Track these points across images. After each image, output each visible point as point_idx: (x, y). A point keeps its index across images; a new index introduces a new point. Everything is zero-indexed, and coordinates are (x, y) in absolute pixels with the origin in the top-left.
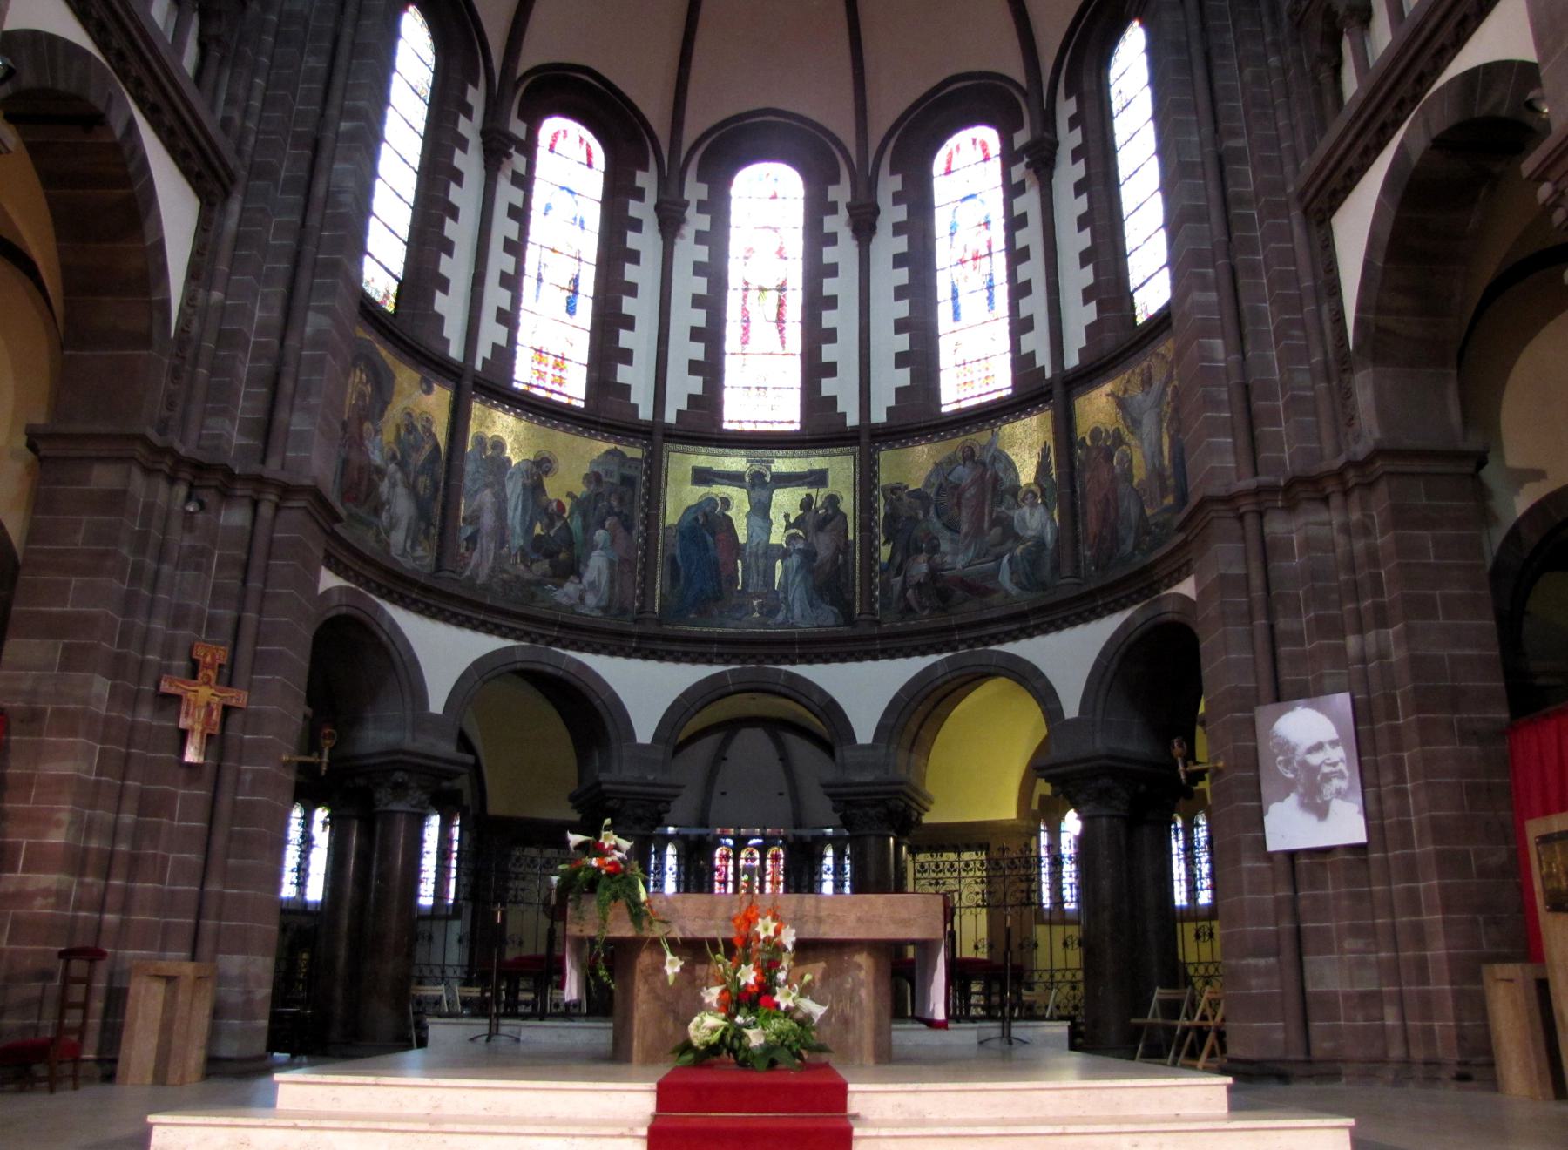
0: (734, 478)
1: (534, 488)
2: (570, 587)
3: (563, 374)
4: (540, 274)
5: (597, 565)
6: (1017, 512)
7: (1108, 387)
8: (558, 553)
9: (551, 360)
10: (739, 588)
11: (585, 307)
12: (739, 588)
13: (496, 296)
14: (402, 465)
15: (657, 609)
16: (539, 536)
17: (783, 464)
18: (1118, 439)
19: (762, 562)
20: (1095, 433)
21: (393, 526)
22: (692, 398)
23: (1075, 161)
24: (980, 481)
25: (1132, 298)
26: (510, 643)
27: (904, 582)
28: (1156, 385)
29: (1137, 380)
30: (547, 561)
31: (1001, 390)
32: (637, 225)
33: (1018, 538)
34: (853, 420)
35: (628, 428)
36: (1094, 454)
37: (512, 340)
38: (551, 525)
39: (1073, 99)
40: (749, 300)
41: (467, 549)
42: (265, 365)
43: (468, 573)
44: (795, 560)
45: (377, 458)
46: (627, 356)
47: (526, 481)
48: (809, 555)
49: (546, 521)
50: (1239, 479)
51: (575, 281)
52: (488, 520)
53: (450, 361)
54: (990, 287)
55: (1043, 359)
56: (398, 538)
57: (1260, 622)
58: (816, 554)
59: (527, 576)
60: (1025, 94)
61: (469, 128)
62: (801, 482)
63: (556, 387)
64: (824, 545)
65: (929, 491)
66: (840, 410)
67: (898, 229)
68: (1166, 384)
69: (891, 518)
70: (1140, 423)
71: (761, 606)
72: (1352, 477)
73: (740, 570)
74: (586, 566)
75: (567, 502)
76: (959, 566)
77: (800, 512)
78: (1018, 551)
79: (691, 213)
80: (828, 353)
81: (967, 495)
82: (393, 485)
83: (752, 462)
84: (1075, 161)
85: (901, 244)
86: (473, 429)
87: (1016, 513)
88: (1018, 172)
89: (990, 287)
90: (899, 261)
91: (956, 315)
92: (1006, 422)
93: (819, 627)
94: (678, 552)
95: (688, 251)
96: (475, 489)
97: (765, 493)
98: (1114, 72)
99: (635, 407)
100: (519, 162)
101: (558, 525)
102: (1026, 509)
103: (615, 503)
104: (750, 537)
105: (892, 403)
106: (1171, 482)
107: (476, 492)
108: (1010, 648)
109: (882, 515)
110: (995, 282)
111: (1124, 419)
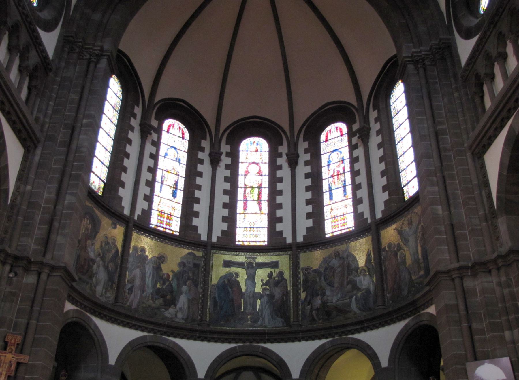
0: (240, 265)
1: (158, 268)
2: (172, 310)
3: (171, 222)
4: (162, 181)
5: (183, 301)
6: (358, 278)
7: (394, 226)
8: (167, 296)
9: (166, 216)
10: (242, 310)
11: (180, 195)
12: (242, 310)
13: (144, 190)
14: (103, 258)
15: (208, 319)
16: (159, 288)
17: (260, 259)
18: (399, 247)
19: (252, 299)
20: (390, 245)
21: (97, 284)
22: (223, 232)
23: (377, 135)
25: (403, 190)
26: (145, 334)
27: (311, 308)
28: (414, 224)
29: (406, 223)
30: (162, 299)
31: (350, 228)
32: (201, 162)
33: (359, 289)
34: (289, 240)
35: (197, 244)
36: (389, 253)
37: (150, 208)
38: (164, 284)
39: (376, 111)
40: (247, 192)
41: (128, 293)
42: (47, 216)
43: (128, 304)
44: (266, 299)
45: (92, 255)
46: (197, 215)
47: (154, 266)
48: (271, 297)
49: (162, 282)
50: (451, 263)
51: (176, 184)
52: (138, 282)
53: (125, 216)
54: (344, 186)
55: (367, 215)
56: (99, 289)
57: (465, 325)
58: (274, 296)
59: (154, 305)
60: (357, 110)
61: (135, 123)
62: (267, 266)
63: (168, 227)
64: (278, 293)
65: (321, 270)
66: (284, 236)
67: (307, 163)
68: (418, 224)
69: (305, 281)
70: (408, 241)
71: (251, 318)
72: (500, 262)
73: (243, 303)
74: (178, 301)
75: (171, 274)
76: (334, 301)
77: (268, 279)
78: (359, 294)
79: (223, 157)
80: (279, 213)
81: (337, 271)
82: (98, 266)
83: (248, 258)
84: (377, 135)
85: (308, 169)
86: (133, 243)
87: (357, 279)
88: (355, 140)
89: (344, 186)
90: (307, 176)
91: (331, 198)
92: (352, 241)
93: (276, 327)
94: (217, 295)
95: (222, 172)
96: (133, 268)
97: (253, 271)
98: (392, 100)
99: (200, 235)
100: (155, 136)
101: (167, 284)
102: (362, 277)
103: (191, 275)
104: (247, 289)
105: (305, 233)
106: (422, 265)
107: (133, 270)
108: (357, 336)
109: (302, 279)
110: (347, 184)
111: (402, 239)
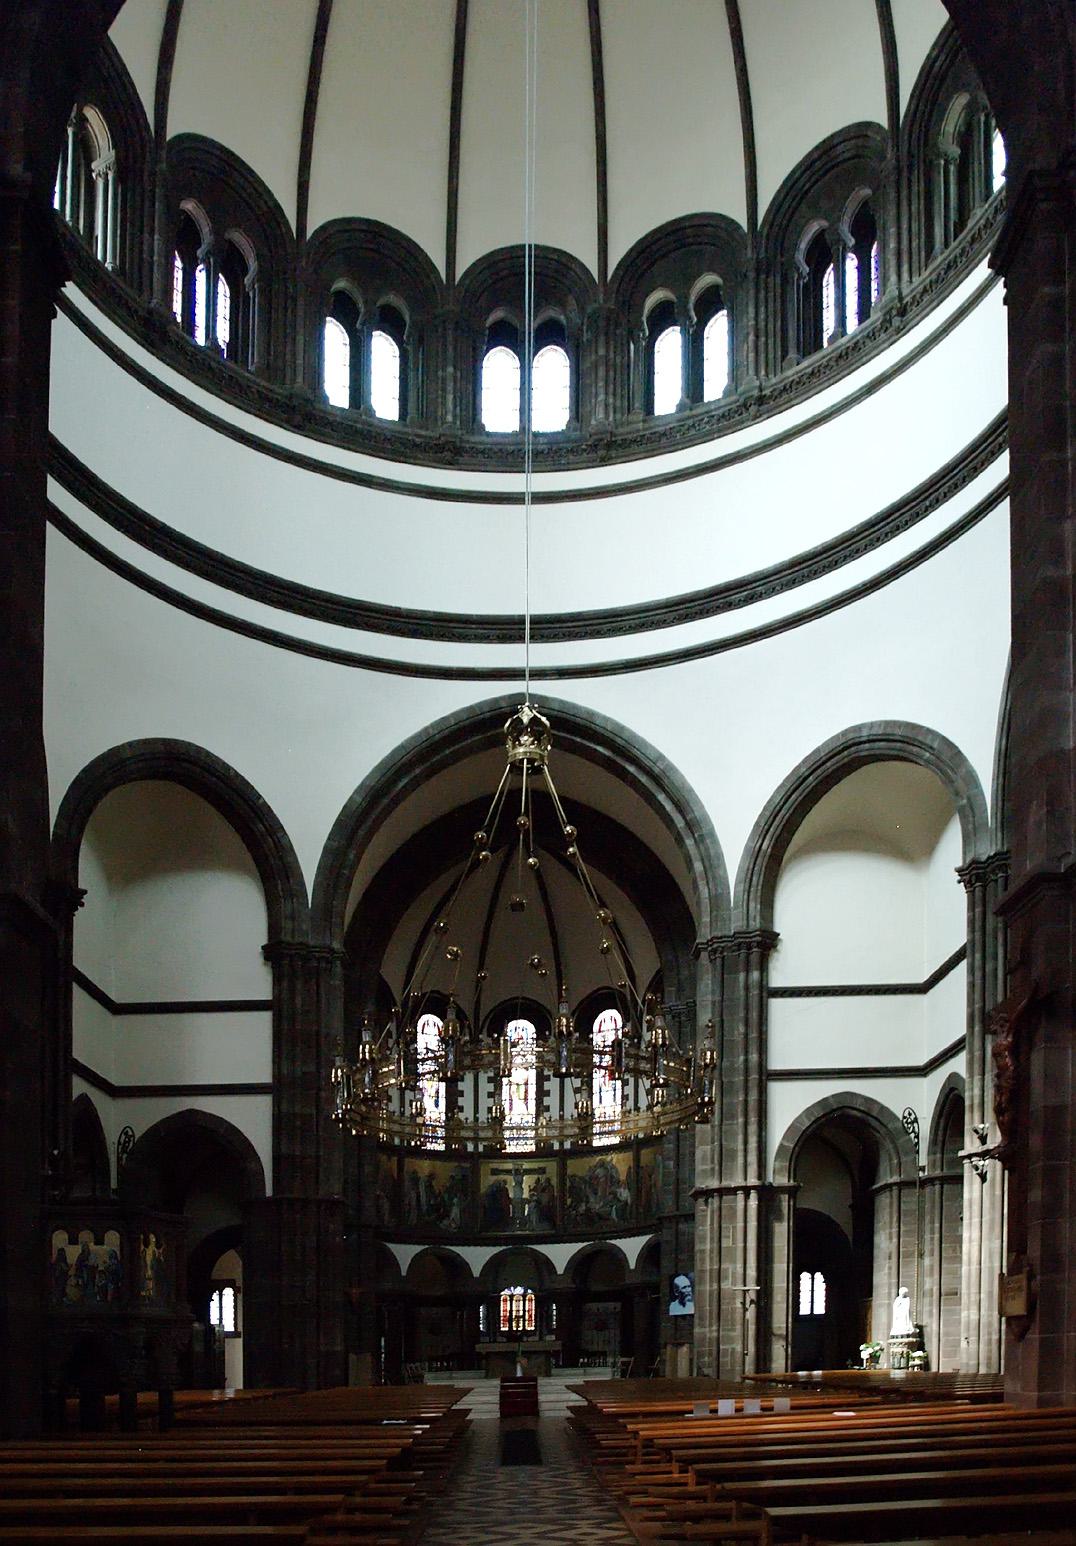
0: (508, 1172)
1: (429, 1186)
17: (526, 1165)
33: (619, 1200)
44: (533, 1204)
48: (538, 1202)
52: (414, 1203)
64: (545, 1199)
69: (572, 1187)
102: (622, 1190)
104: (515, 1195)
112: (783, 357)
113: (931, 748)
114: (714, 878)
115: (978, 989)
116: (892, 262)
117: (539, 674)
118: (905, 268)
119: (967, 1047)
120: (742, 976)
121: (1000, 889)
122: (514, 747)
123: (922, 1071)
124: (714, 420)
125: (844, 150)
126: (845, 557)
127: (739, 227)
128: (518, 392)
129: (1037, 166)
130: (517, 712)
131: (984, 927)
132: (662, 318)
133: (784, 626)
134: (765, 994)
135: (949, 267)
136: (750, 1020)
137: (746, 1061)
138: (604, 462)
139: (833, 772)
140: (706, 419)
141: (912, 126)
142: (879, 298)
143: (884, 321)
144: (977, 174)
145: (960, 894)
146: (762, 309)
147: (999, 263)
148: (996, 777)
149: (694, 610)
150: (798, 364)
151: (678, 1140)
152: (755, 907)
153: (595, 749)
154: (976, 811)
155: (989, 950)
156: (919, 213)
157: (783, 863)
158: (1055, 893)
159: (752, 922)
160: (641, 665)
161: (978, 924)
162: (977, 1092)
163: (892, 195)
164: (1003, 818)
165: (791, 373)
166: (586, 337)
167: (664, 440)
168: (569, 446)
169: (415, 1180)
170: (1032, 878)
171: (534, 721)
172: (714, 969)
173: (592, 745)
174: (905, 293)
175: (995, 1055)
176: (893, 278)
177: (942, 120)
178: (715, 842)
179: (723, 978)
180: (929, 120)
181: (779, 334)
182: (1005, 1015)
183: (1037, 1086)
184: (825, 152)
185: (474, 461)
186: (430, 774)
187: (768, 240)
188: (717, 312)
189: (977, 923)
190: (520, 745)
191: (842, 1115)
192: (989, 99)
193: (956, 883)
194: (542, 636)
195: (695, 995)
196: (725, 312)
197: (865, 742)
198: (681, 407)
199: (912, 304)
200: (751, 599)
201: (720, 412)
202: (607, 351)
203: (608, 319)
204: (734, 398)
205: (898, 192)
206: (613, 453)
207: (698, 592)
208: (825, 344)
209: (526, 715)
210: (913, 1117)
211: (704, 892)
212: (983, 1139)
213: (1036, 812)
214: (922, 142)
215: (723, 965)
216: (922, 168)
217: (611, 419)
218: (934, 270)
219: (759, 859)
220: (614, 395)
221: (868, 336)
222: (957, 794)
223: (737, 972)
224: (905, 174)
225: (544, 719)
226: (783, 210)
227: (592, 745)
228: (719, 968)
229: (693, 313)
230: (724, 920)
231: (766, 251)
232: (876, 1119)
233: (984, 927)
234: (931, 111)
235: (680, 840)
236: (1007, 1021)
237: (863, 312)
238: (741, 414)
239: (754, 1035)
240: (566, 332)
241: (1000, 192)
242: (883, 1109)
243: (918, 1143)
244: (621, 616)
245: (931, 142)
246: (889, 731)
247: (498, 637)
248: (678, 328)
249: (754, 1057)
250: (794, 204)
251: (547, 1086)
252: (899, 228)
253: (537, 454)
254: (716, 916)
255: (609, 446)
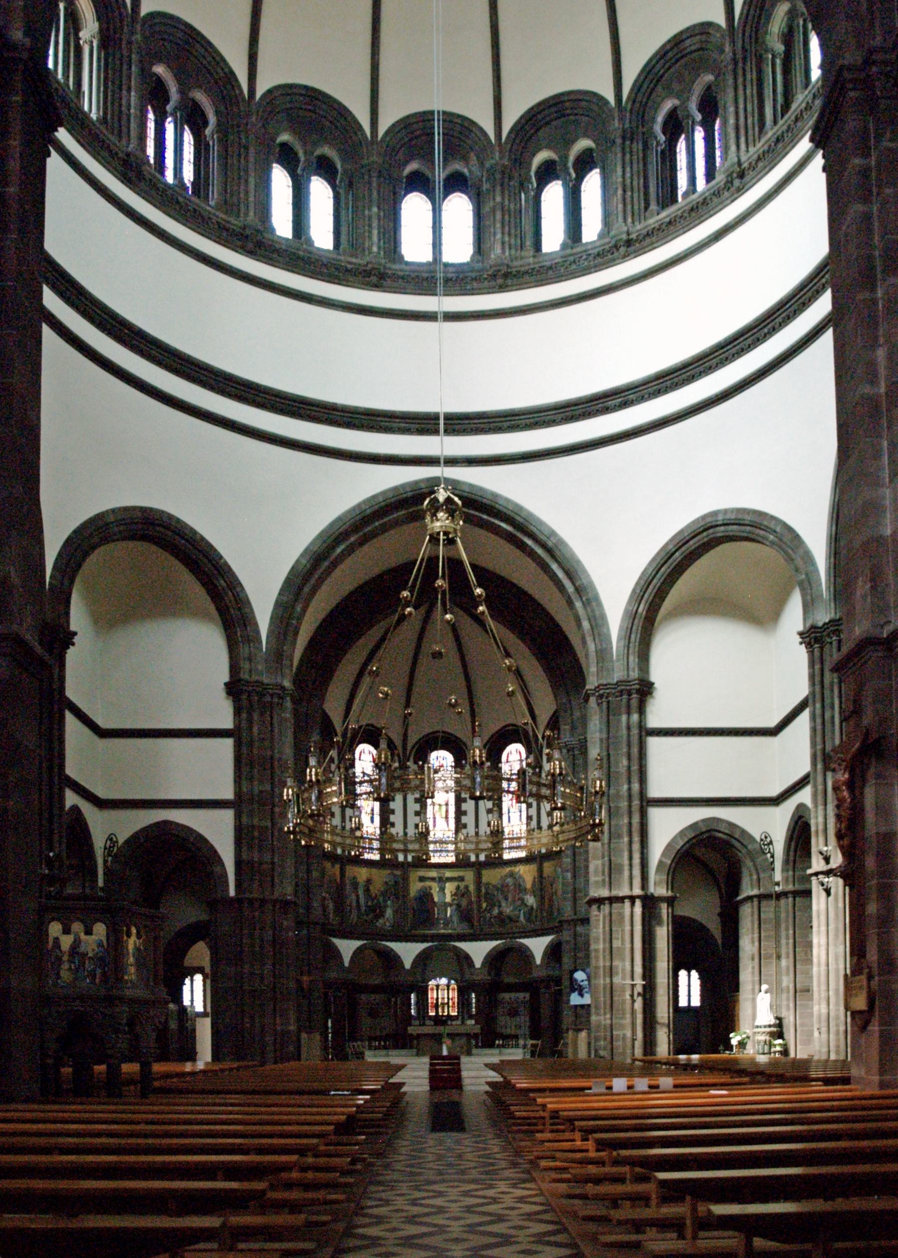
0: (433, 879)
1: (367, 890)
2: (381, 921)
5: (389, 913)
17: (448, 874)
24: (515, 884)
33: (526, 906)
44: (454, 907)
48: (459, 905)
52: (354, 904)
64: (464, 902)
69: (487, 893)
78: (526, 909)
112: (646, 208)
113: (775, 531)
114: (599, 635)
115: (819, 733)
116: (732, 135)
117: (452, 462)
118: (743, 140)
119: (811, 782)
120: (624, 718)
121: (835, 650)
122: (432, 521)
123: (776, 801)
124: (591, 258)
125: (691, 44)
126: (701, 373)
127: (607, 102)
128: (431, 230)
129: (846, 63)
130: (434, 492)
131: (822, 682)
132: (548, 173)
133: (652, 428)
134: (643, 734)
135: (778, 140)
136: (632, 755)
137: (629, 789)
138: (502, 288)
139: (695, 549)
140: (584, 257)
141: (745, 26)
142: (722, 164)
143: (727, 182)
144: (798, 68)
145: (802, 653)
146: (628, 169)
147: (818, 138)
148: (829, 557)
149: (577, 413)
150: (658, 214)
151: (574, 854)
152: (633, 660)
153: (499, 526)
154: (814, 585)
155: (827, 701)
156: (752, 96)
157: (656, 624)
158: (880, 654)
159: (631, 673)
160: (535, 457)
161: (818, 679)
162: (821, 819)
163: (731, 81)
164: (835, 591)
165: (653, 221)
166: (485, 186)
167: (550, 272)
168: (474, 275)
169: (355, 885)
170: (861, 641)
171: (449, 500)
172: (601, 711)
173: (497, 522)
174: (743, 159)
175: (836, 789)
176: (733, 148)
177: (768, 23)
178: (600, 605)
179: (608, 720)
180: (758, 23)
181: (642, 189)
182: (842, 756)
183: (870, 816)
184: (676, 45)
185: (395, 284)
186: (362, 542)
187: (631, 113)
188: (591, 169)
189: (816, 678)
190: (437, 520)
191: (709, 837)
192: (806, 7)
193: (798, 644)
194: (454, 430)
195: (585, 733)
196: (597, 170)
197: (721, 525)
198: (564, 246)
199: (749, 169)
200: (625, 405)
201: (596, 251)
202: (503, 199)
203: (503, 173)
204: (607, 240)
205: (735, 79)
206: (509, 282)
207: (580, 398)
208: (680, 199)
209: (442, 496)
210: (768, 840)
211: (591, 646)
212: (827, 860)
213: (862, 587)
214: (753, 40)
215: (608, 708)
216: (753, 63)
217: (507, 254)
218: (766, 142)
219: (636, 620)
220: (509, 234)
221: (714, 194)
222: (797, 570)
223: (620, 714)
224: (740, 65)
225: (456, 499)
226: (643, 90)
227: (497, 522)
228: (605, 710)
229: (572, 171)
230: (608, 670)
231: (630, 122)
232: (738, 841)
233: (822, 682)
234: (760, 15)
235: (570, 603)
236: (843, 761)
237: (710, 174)
238: (612, 254)
239: (635, 768)
240: (470, 183)
241: (817, 82)
242: (744, 832)
243: (773, 863)
244: (518, 415)
245: (760, 40)
246: (740, 516)
247: (417, 430)
248: (560, 182)
249: (636, 786)
250: (652, 86)
251: (464, 806)
252: (737, 108)
253: (447, 280)
254: (602, 667)
255: (506, 275)
